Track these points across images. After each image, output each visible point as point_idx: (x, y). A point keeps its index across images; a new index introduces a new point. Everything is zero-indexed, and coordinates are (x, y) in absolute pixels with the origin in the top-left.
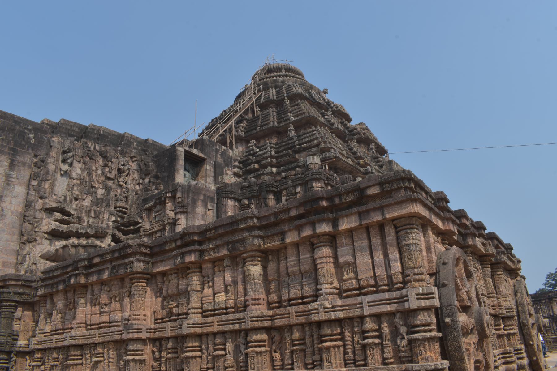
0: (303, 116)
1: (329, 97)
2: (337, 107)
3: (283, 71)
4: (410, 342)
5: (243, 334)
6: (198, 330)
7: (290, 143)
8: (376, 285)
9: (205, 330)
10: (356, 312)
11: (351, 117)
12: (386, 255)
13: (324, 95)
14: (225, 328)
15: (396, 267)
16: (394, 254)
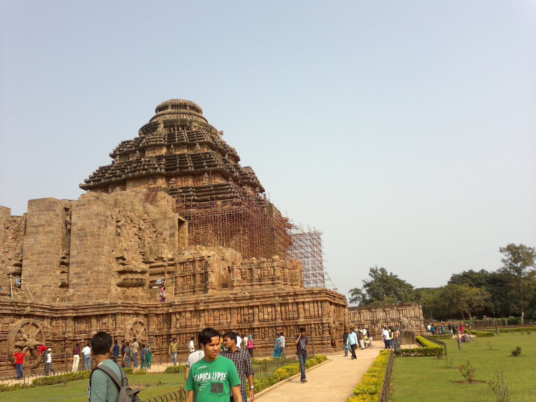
0: (216, 168)
1: (223, 138)
2: (232, 151)
3: (188, 108)
4: (322, 330)
5: (275, 327)
6: (260, 326)
7: (207, 191)
8: (315, 316)
9: (262, 326)
10: (310, 323)
11: (240, 158)
12: (318, 308)
13: (220, 135)
14: (268, 326)
15: (320, 312)
16: (320, 309)
